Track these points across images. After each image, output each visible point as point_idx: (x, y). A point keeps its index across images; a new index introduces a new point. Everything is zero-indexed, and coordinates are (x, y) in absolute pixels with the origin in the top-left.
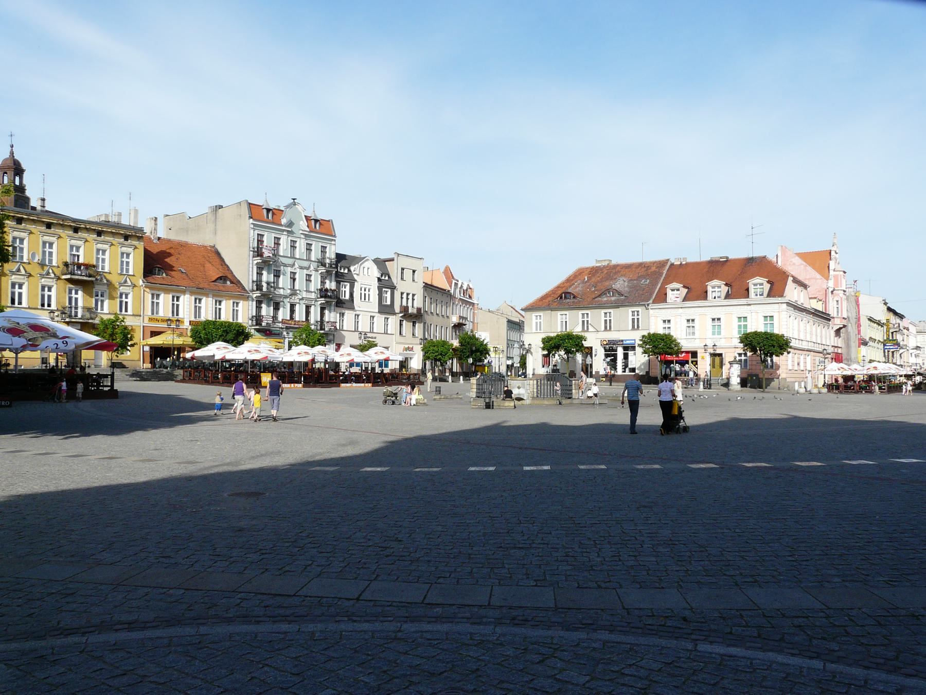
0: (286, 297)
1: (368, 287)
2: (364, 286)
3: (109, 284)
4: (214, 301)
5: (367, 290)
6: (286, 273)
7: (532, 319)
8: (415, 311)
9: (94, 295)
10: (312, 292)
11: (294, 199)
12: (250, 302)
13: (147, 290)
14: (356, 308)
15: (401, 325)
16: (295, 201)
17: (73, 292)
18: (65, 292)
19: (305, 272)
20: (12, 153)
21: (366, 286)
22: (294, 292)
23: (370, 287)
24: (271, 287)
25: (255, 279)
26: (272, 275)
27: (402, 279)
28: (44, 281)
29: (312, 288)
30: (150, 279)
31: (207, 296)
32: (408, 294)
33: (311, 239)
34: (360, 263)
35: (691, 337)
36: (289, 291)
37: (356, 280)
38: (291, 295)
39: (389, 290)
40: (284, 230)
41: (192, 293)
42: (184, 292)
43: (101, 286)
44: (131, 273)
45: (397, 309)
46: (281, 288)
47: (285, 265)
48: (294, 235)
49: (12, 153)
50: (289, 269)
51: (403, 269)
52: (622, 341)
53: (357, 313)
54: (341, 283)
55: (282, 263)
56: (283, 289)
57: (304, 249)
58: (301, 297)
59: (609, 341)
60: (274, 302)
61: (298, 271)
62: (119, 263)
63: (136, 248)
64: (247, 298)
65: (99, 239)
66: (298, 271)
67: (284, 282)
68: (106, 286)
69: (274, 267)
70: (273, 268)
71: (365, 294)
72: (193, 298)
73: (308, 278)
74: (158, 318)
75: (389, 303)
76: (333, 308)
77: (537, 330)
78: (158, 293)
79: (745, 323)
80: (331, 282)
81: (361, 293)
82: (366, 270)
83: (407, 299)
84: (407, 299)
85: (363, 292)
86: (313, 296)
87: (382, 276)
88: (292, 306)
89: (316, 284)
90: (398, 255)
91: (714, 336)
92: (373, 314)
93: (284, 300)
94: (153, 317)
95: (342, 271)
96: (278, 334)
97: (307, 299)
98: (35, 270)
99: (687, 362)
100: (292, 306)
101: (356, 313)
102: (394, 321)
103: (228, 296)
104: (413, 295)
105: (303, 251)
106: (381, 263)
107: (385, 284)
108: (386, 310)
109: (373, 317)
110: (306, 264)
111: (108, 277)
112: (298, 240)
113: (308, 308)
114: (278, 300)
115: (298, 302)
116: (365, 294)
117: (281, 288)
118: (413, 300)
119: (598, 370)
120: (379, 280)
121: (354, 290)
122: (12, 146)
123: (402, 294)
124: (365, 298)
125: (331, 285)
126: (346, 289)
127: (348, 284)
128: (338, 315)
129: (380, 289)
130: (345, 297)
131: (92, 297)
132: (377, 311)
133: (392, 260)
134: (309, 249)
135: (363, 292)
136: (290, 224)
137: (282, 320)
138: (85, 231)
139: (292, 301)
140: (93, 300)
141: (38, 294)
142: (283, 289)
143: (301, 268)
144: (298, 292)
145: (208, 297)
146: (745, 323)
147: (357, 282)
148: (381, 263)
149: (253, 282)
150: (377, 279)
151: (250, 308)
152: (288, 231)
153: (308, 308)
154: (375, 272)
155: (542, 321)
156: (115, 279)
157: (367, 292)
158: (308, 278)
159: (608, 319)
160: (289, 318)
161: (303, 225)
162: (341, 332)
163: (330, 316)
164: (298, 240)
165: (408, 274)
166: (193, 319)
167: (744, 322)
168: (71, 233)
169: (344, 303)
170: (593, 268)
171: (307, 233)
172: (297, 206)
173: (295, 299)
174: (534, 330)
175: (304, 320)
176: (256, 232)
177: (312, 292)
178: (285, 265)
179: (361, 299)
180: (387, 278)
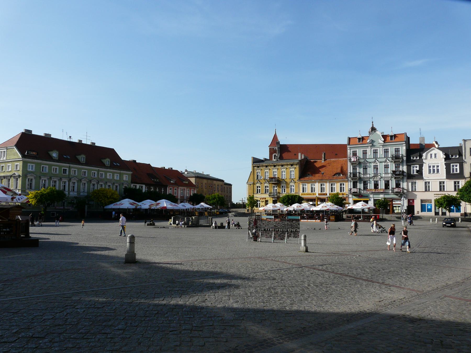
0: (371, 178)
3: (286, 183)
4: (330, 184)
6: (371, 166)
9: (281, 187)
10: (389, 173)
12: (349, 183)
13: (301, 183)
14: (425, 178)
17: (275, 187)
18: (272, 187)
19: (384, 164)
20: (373, 125)
22: (376, 175)
25: (352, 172)
26: (362, 169)
28: (266, 185)
29: (390, 171)
30: (302, 179)
31: (326, 182)
33: (387, 146)
36: (373, 175)
37: (424, 163)
38: (374, 176)
39: (458, 164)
40: (368, 146)
41: (319, 182)
42: (316, 182)
43: (283, 184)
44: (294, 178)
46: (368, 174)
47: (370, 163)
48: (376, 147)
49: (373, 126)
50: (373, 164)
56: (369, 174)
58: (380, 177)
61: (378, 164)
62: (289, 175)
63: (295, 168)
64: (348, 181)
65: (282, 167)
66: (378, 164)
67: (371, 171)
68: (285, 184)
69: (363, 164)
70: (362, 165)
72: (320, 184)
73: (386, 167)
74: (305, 193)
76: (405, 180)
78: (334, 183)
80: (403, 166)
82: (433, 156)
85: (431, 168)
86: (390, 175)
90: (465, 141)
93: (370, 179)
94: (303, 193)
95: (415, 159)
96: (367, 196)
97: (385, 177)
98: (263, 181)
101: (425, 181)
103: (337, 181)
109: (444, 182)
111: (286, 180)
114: (366, 180)
115: (379, 179)
117: (368, 174)
121: (423, 168)
122: (373, 122)
125: (404, 168)
128: (410, 184)
131: (280, 188)
132: (445, 178)
134: (386, 151)
135: (431, 168)
136: (372, 142)
138: (278, 166)
139: (375, 179)
140: (281, 189)
141: (264, 189)
142: (369, 174)
144: (379, 175)
145: (327, 183)
147: (425, 163)
149: (350, 173)
150: (444, 159)
151: (349, 185)
156: (288, 181)
157: (435, 168)
158: (386, 167)
161: (381, 140)
162: (414, 193)
163: (404, 185)
164: (378, 149)
166: (320, 192)
168: (273, 167)
169: (415, 177)
171: (383, 144)
172: (376, 132)
173: (377, 179)
176: (352, 150)
177: (389, 173)
178: (370, 163)
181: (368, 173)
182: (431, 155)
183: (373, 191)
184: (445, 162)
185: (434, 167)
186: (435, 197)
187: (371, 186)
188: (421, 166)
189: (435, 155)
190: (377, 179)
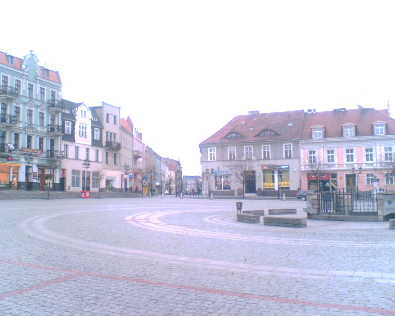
1: (85, 126)
2: (82, 125)
5: (84, 128)
7: (207, 151)
8: (116, 145)
10: (44, 127)
11: (31, 51)
15: (107, 156)
16: (32, 52)
21: (83, 125)
23: (86, 126)
24: (13, 120)
27: (108, 121)
32: (111, 133)
34: (79, 107)
35: (331, 163)
37: (76, 120)
39: (99, 129)
40: (23, 75)
45: (104, 143)
51: (108, 115)
52: (279, 166)
53: (78, 145)
54: (66, 121)
55: (22, 102)
57: (38, 92)
59: (268, 166)
60: (14, 133)
71: (83, 131)
75: (99, 138)
77: (211, 159)
79: (352, 154)
81: (80, 131)
83: (111, 136)
84: (111, 136)
86: (45, 130)
87: (93, 119)
88: (29, 139)
89: (47, 120)
91: (348, 163)
92: (88, 147)
99: (328, 181)
100: (29, 139)
102: (102, 152)
104: (115, 134)
105: (37, 93)
106: (94, 110)
107: (97, 124)
108: (96, 143)
110: (39, 104)
112: (34, 84)
113: (41, 140)
116: (83, 131)
118: (115, 137)
119: (260, 188)
120: (93, 122)
123: (107, 132)
124: (83, 135)
126: (68, 127)
127: (71, 122)
129: (93, 128)
130: (68, 132)
132: (90, 144)
133: (101, 107)
137: (22, 148)
143: (37, 107)
146: (352, 154)
148: (94, 110)
152: (27, 76)
153: (41, 140)
154: (89, 115)
155: (215, 152)
159: (266, 151)
160: (26, 147)
165: (111, 119)
167: (351, 153)
170: (247, 116)
171: (41, 79)
174: (209, 159)
175: (38, 148)
179: (80, 135)
180: (97, 120)
181: (21, 120)
182: (82, 111)
183: (28, 152)
184: (92, 125)
185: (83, 128)
186: (83, 167)
187: (23, 142)
188: (73, 124)
189: (85, 112)
190: (30, 132)
